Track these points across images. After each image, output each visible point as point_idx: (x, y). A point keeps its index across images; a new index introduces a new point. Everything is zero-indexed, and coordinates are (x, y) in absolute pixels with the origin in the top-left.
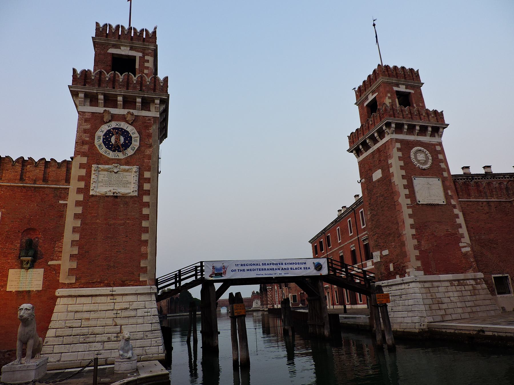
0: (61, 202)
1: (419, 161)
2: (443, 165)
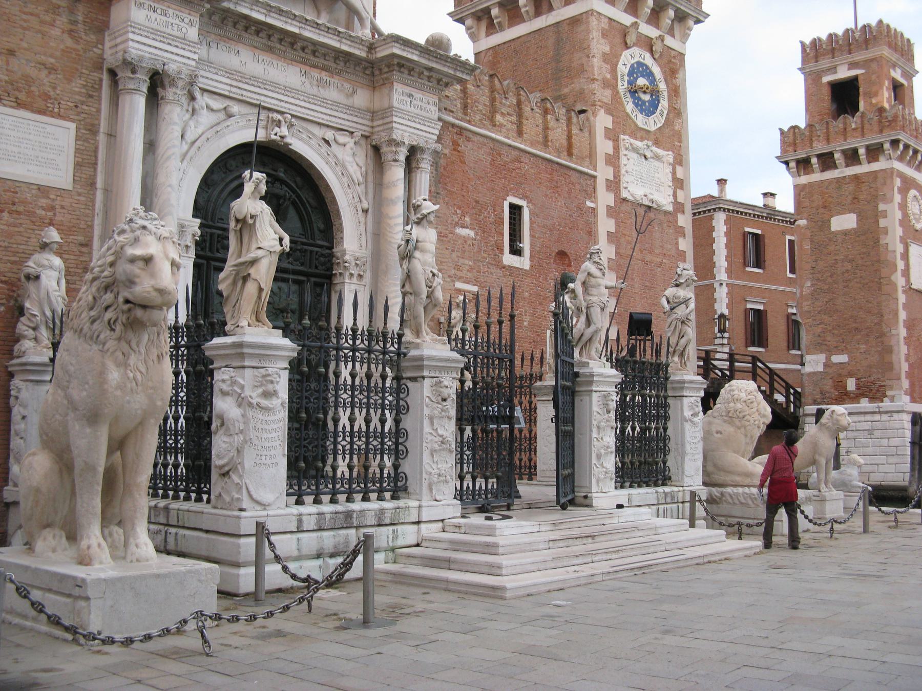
0: (589, 204)
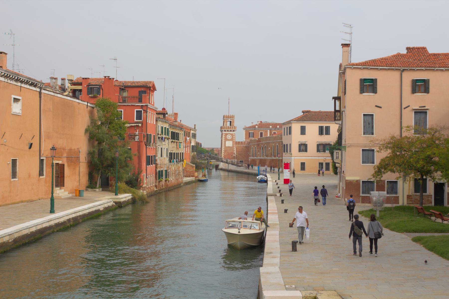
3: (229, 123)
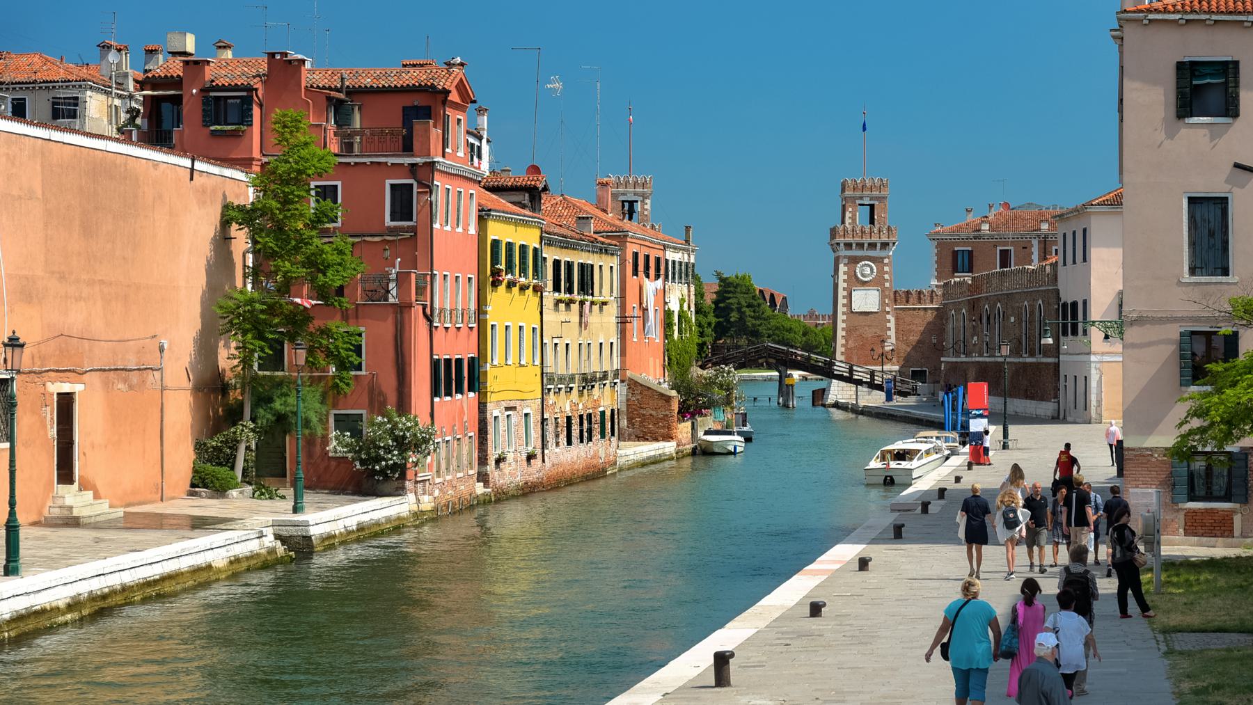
1: (863, 275)
2: (887, 277)
3: (861, 215)
